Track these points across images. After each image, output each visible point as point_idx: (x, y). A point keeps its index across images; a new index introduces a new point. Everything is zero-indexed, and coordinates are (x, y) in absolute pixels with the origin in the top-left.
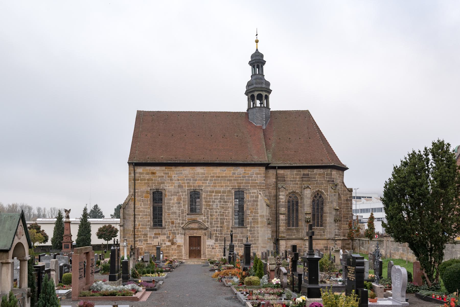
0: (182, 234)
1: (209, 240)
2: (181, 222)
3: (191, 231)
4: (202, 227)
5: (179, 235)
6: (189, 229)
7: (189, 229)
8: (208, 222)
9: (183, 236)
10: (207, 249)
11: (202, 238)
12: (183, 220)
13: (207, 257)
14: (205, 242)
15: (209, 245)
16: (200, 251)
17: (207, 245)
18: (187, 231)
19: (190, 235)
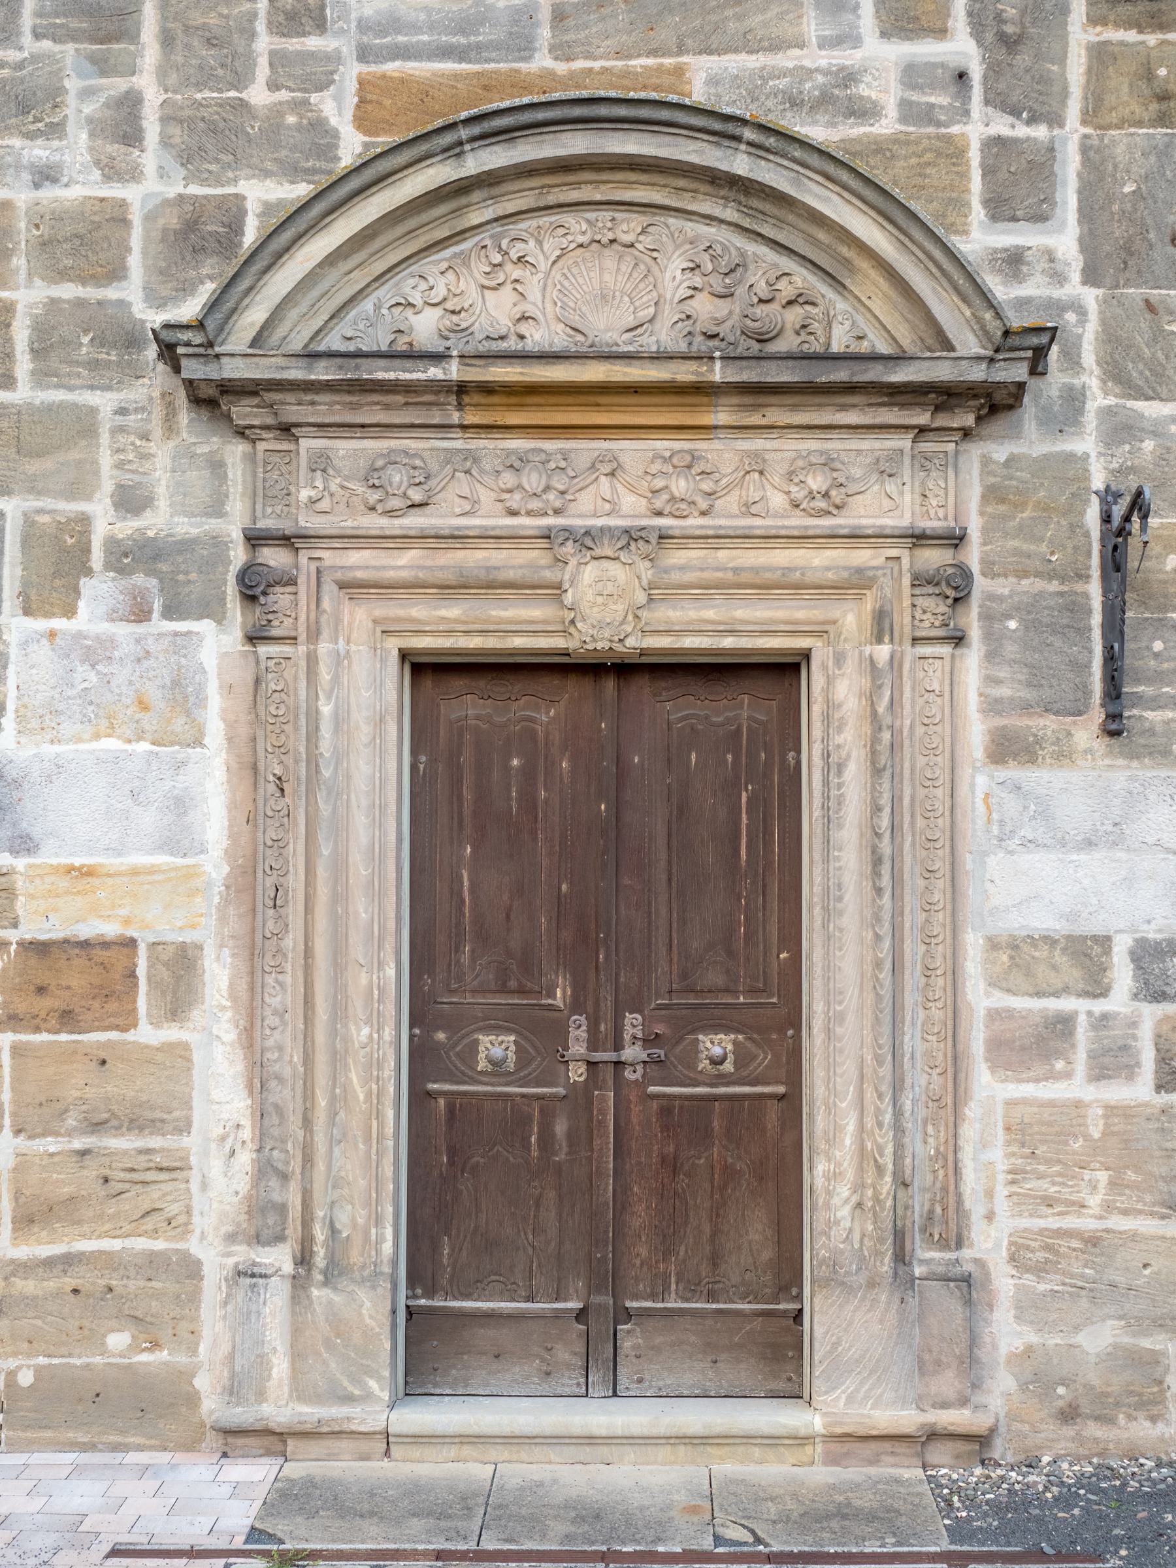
0: (162, 575)
1: (1082, 779)
2: (155, 183)
3: (481, 490)
4: (854, 322)
5: (99, 592)
6: (376, 389)
7: (376, 389)
8: (1019, 185)
9: (216, 643)
10: (990, 1089)
11: (836, 696)
12: (212, 137)
13: (1007, 1333)
14: (921, 859)
15: (1087, 955)
16: (760, 1143)
17: (1017, 955)
18: (333, 480)
19: (451, 628)
